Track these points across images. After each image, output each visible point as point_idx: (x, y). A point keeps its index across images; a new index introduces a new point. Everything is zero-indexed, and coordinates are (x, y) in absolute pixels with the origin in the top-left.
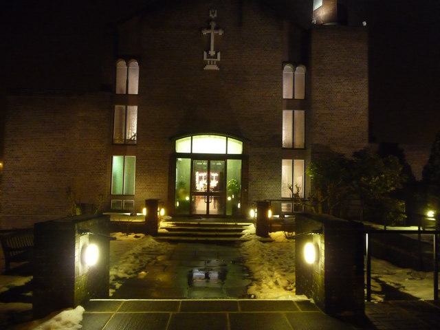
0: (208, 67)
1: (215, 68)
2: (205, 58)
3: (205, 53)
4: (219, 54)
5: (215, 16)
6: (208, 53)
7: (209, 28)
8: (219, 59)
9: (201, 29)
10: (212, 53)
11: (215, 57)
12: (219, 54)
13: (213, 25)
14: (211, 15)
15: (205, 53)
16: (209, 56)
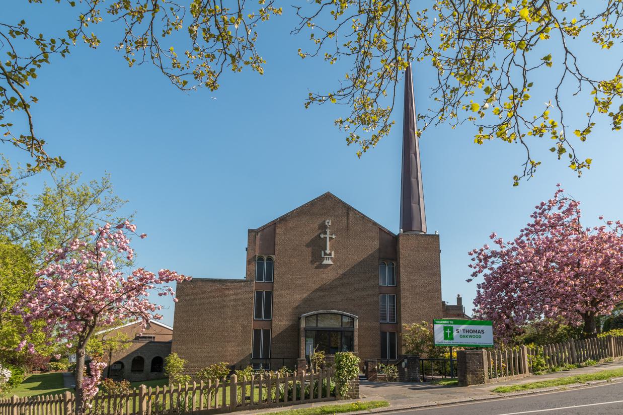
0: (325, 262)
1: (330, 262)
2: (323, 256)
3: (323, 252)
4: (333, 253)
5: (330, 224)
6: (325, 252)
7: (326, 234)
8: (333, 256)
9: (320, 234)
10: (328, 252)
11: (330, 254)
12: (333, 253)
13: (328, 231)
14: (326, 224)
15: (323, 252)
16: (325, 254)
